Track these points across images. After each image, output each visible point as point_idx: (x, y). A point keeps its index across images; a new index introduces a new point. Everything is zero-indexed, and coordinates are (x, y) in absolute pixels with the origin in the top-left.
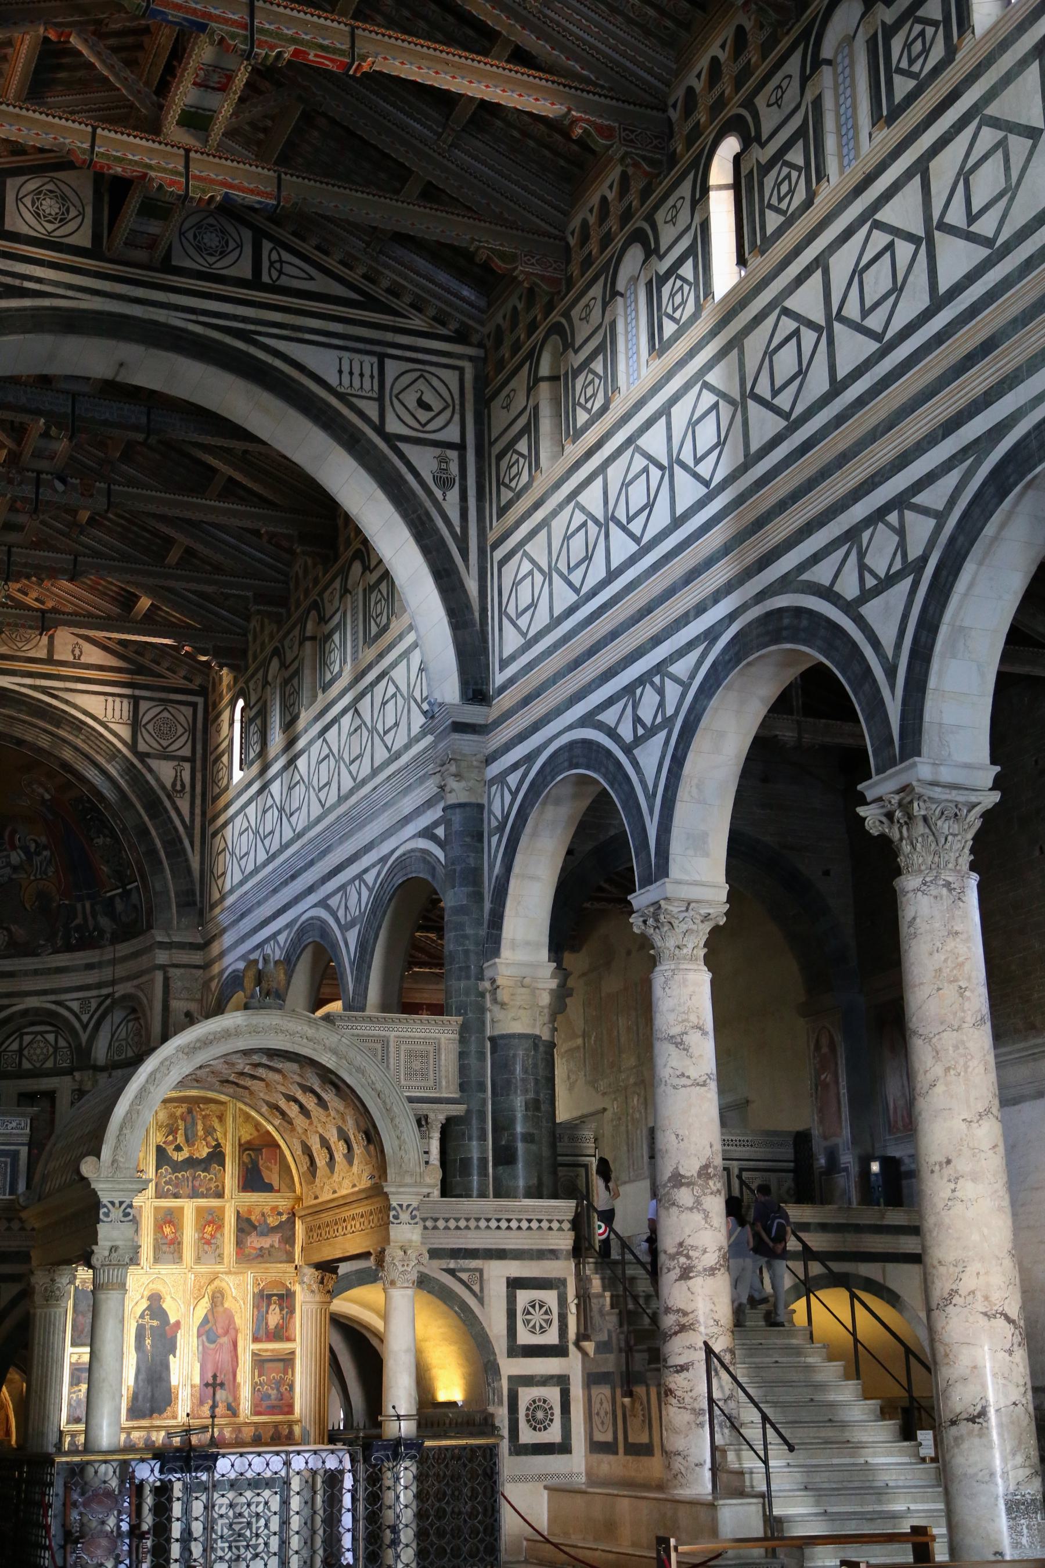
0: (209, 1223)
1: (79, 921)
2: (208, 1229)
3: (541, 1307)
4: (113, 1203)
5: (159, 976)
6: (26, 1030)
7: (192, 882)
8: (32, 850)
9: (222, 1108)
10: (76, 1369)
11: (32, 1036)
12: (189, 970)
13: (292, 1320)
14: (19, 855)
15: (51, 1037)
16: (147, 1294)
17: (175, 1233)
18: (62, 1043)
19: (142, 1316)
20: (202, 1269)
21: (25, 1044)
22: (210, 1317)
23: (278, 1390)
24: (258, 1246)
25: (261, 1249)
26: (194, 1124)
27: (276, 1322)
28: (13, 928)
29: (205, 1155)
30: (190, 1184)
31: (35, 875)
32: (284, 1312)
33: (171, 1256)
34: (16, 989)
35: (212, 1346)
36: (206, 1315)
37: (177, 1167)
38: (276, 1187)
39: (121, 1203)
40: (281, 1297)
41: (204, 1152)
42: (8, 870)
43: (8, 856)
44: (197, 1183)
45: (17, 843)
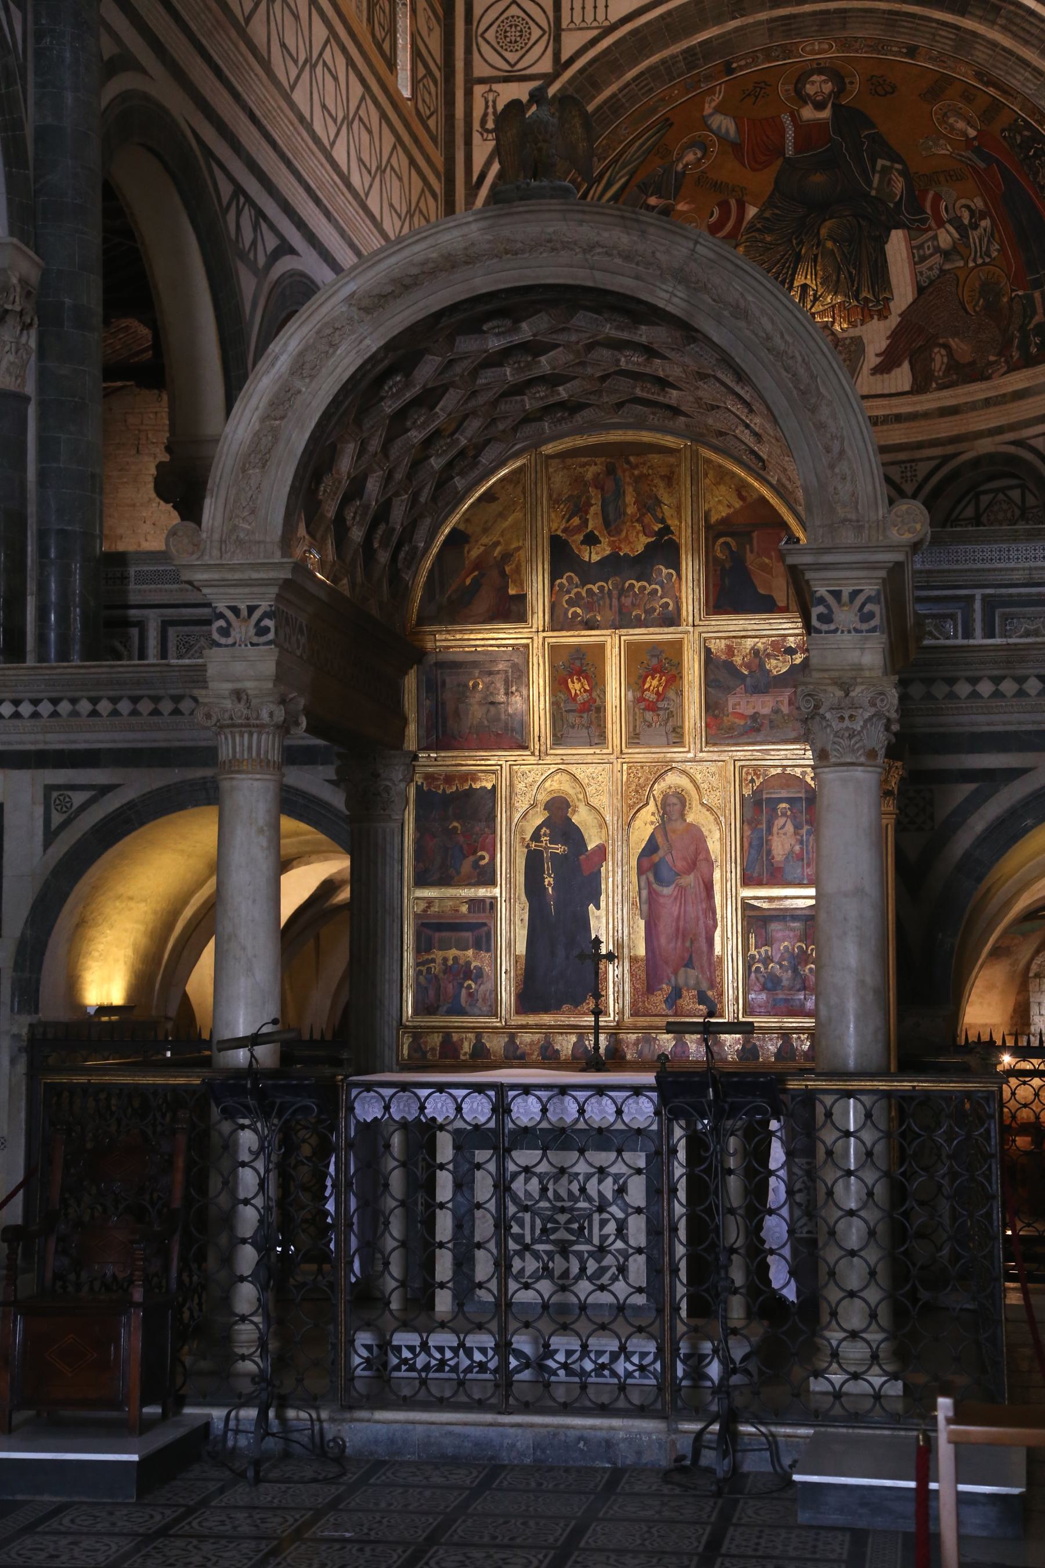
0: (653, 672)
2: (652, 683)
4: (235, 610)
6: (982, 488)
8: (966, 222)
9: (672, 460)
10: (423, 925)
11: (991, 496)
14: (947, 231)
15: (1015, 494)
16: (543, 797)
17: (590, 692)
18: (1031, 500)
19: (536, 836)
20: (640, 755)
21: (982, 506)
22: (660, 840)
23: (795, 971)
24: (750, 712)
25: (755, 717)
26: (619, 494)
27: (787, 847)
28: (953, 342)
29: (640, 549)
30: (615, 602)
31: (974, 260)
32: (804, 831)
33: (584, 733)
34: (963, 430)
36: (652, 837)
37: (587, 573)
38: (781, 602)
39: (251, 609)
41: (640, 543)
42: (937, 259)
43: (935, 238)
44: (627, 601)
45: (944, 214)
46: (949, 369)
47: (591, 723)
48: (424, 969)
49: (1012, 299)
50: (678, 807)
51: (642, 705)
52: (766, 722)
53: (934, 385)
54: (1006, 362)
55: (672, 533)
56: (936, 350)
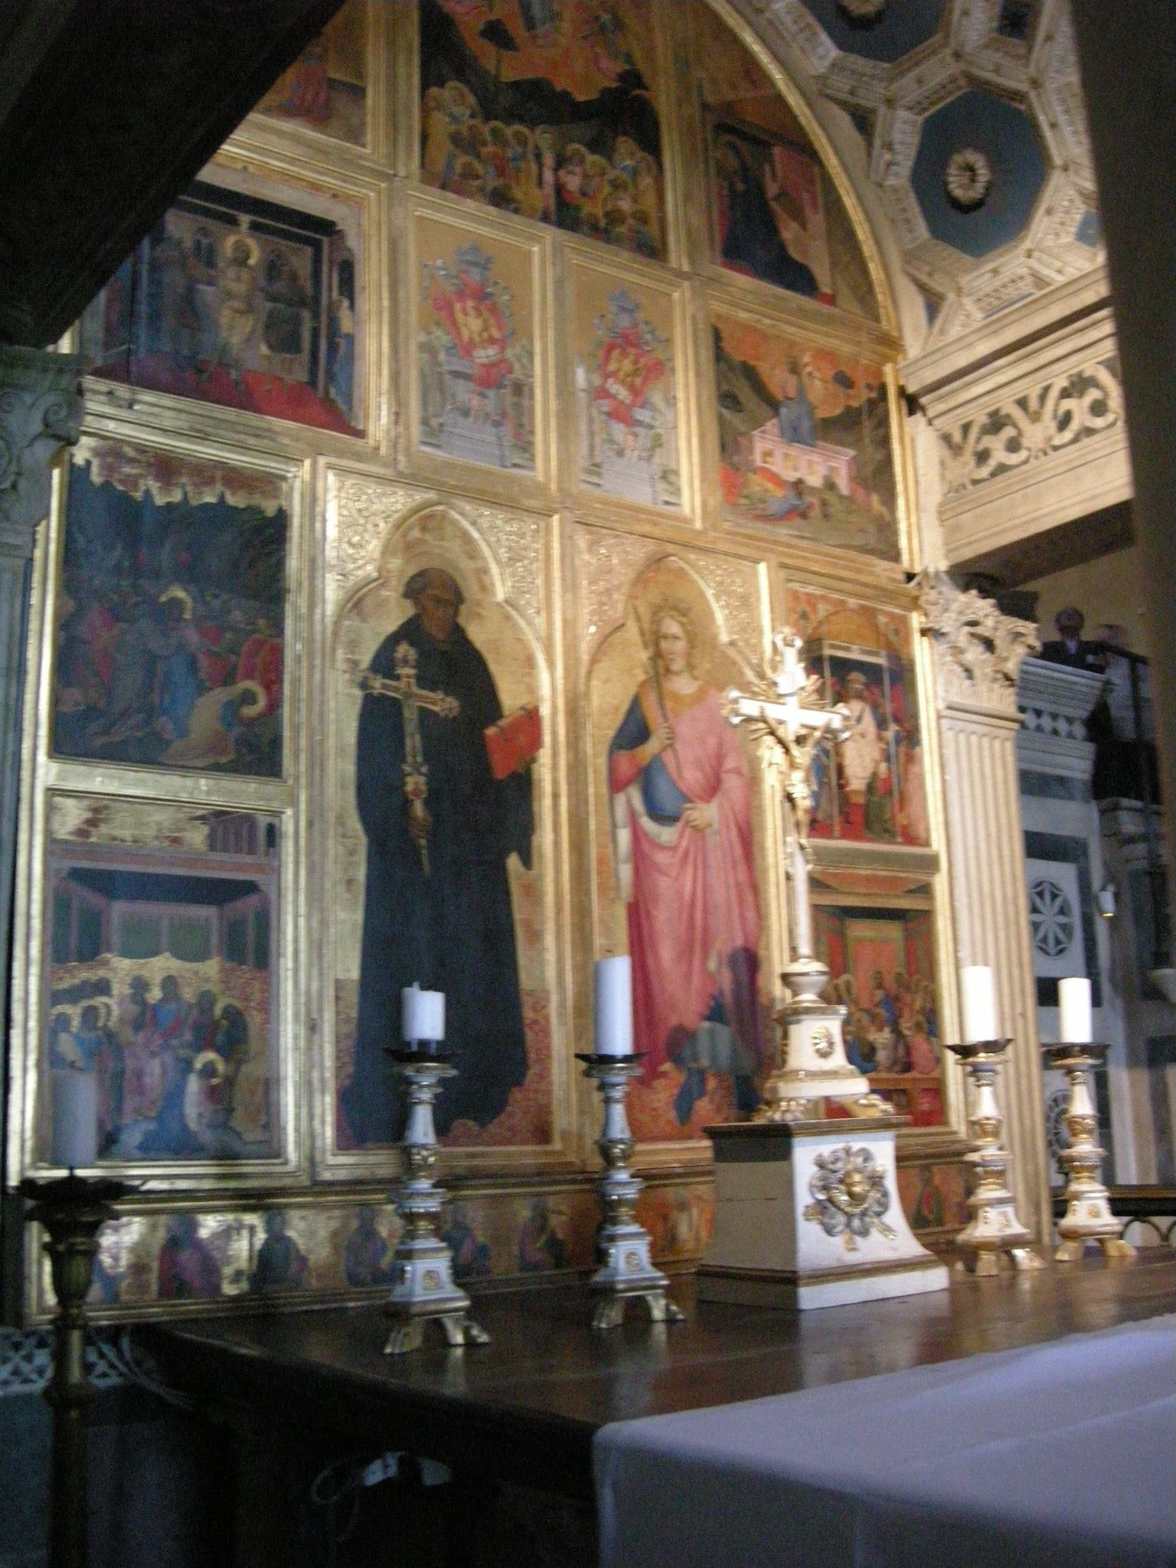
3: (1054, 896)
10: (77, 874)
13: (914, 769)
19: (384, 663)
23: (897, 1031)
24: (791, 476)
29: (594, 95)
30: (549, 176)
33: (489, 434)
35: (667, 834)
36: (636, 705)
40: (872, 672)
47: (504, 415)
48: (73, 1012)
50: (681, 645)
51: (606, 405)
52: (815, 501)
55: (646, 88)
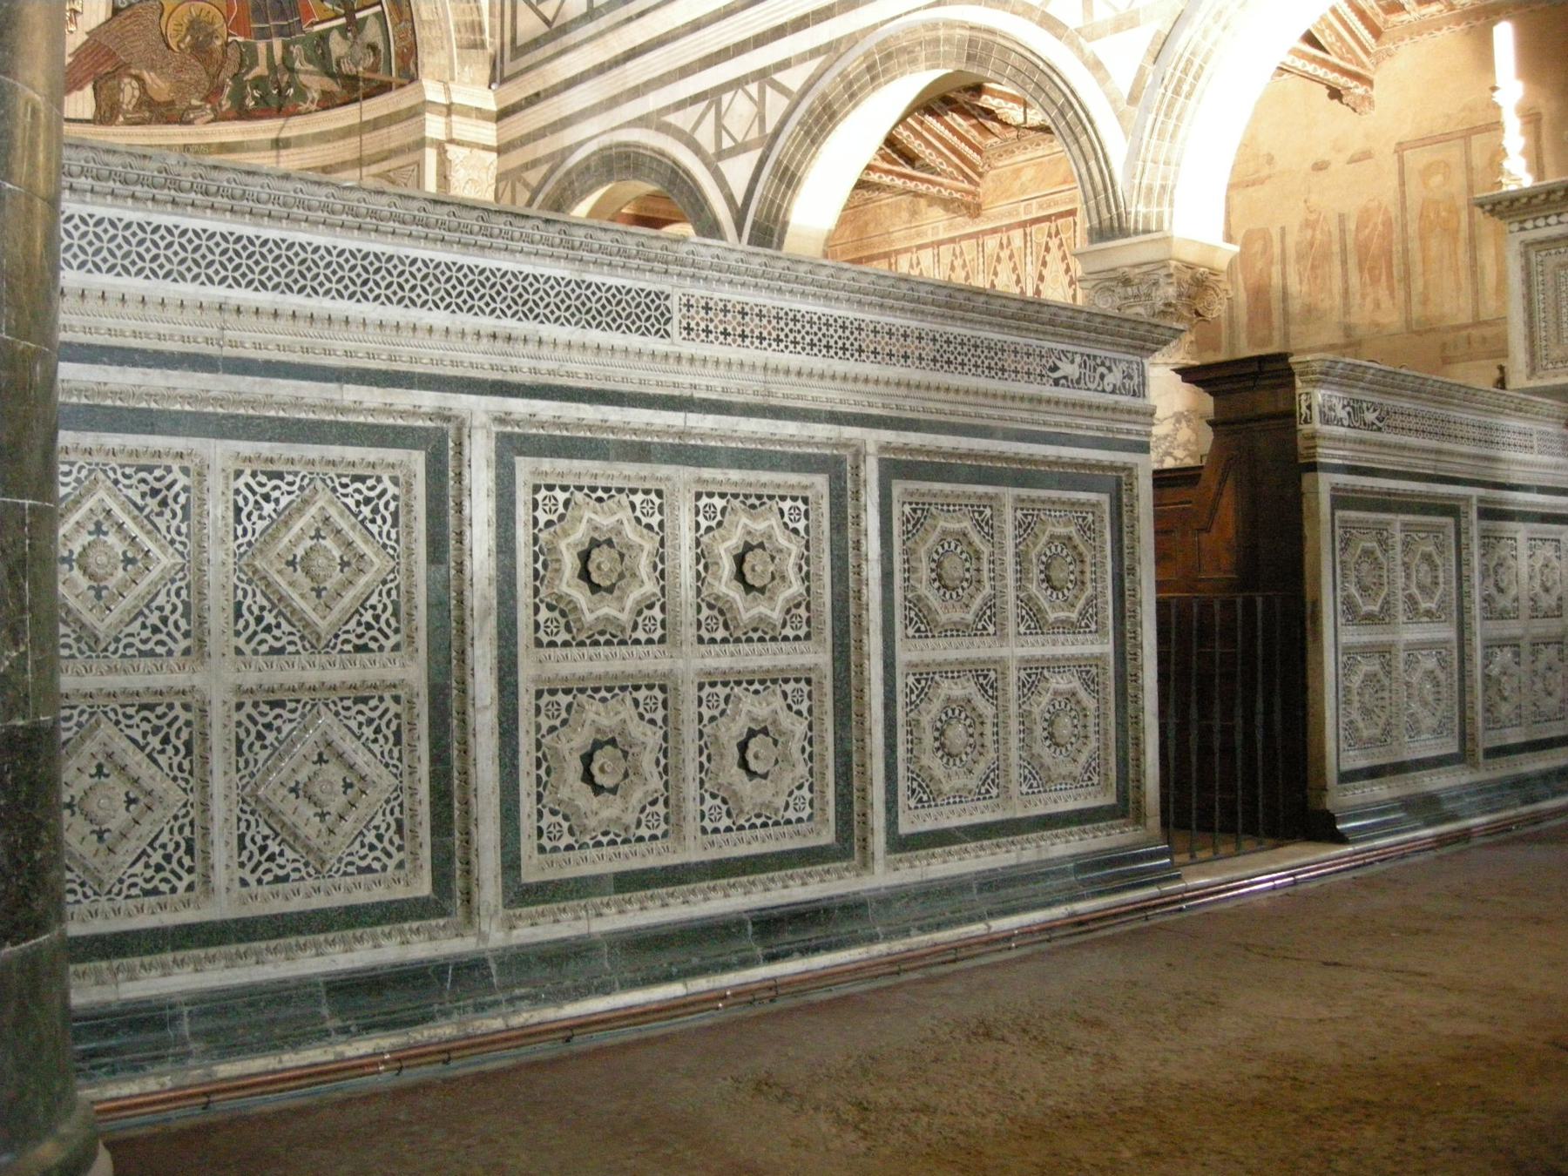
1: (257, 71)
5: (431, 156)
7: (478, 9)
12: (476, 151)
28: (148, 76)
46: (139, 105)
49: (227, 44)
53: (121, 118)
54: (213, 109)
56: (127, 80)
